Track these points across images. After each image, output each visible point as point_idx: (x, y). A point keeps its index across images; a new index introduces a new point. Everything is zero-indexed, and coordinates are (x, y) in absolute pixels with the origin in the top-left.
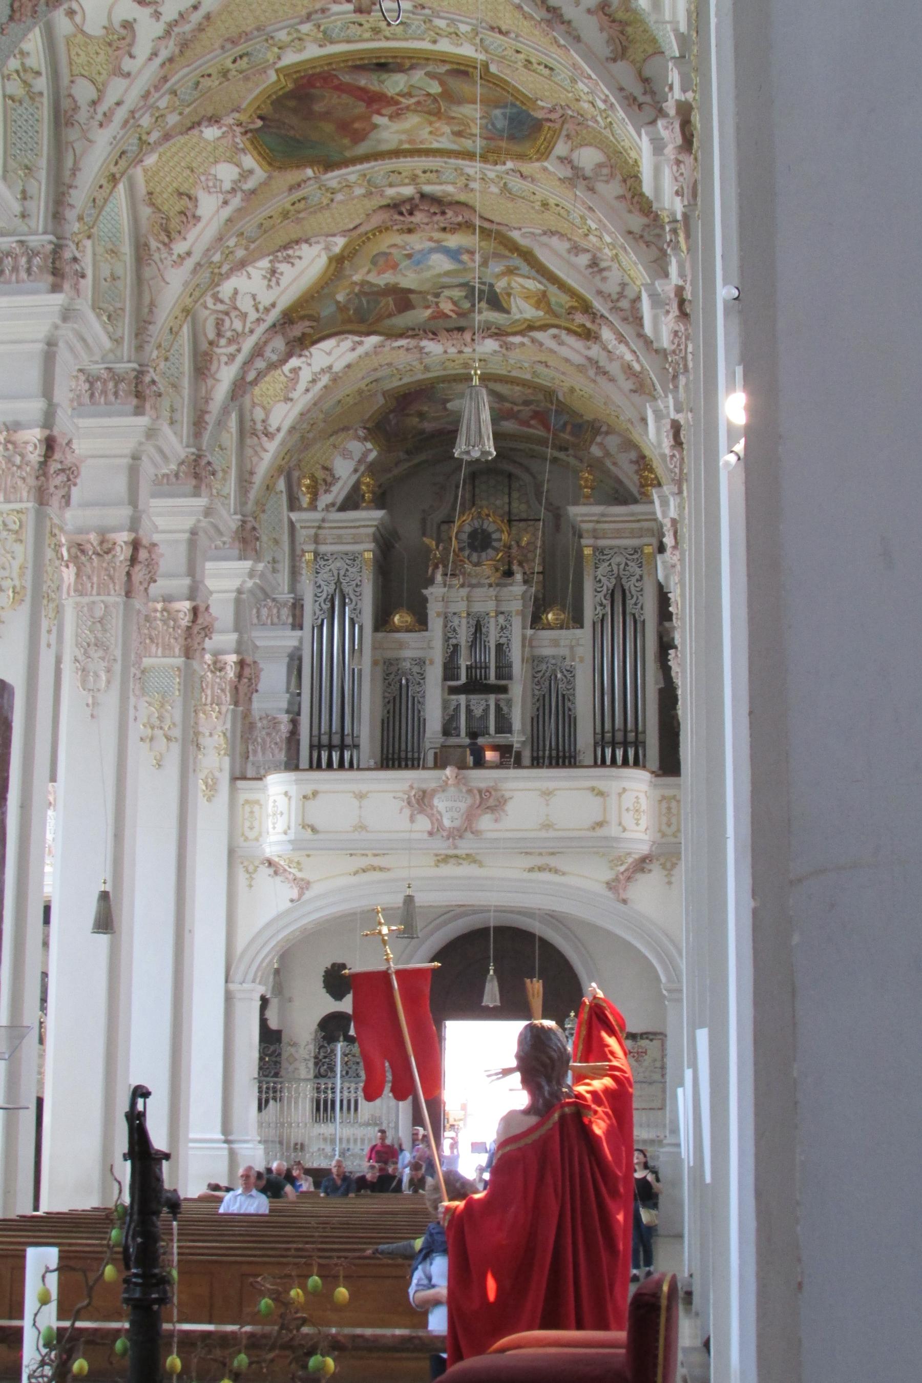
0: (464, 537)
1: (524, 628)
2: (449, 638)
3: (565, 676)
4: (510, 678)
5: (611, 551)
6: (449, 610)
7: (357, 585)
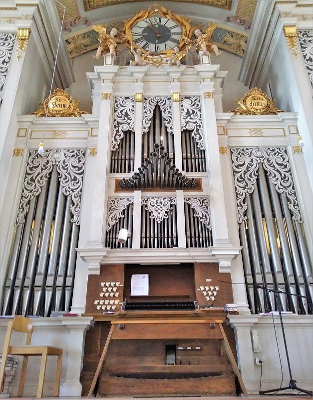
0: (140, 31)
1: (217, 111)
2: (118, 123)
3: (277, 170)
4: (203, 168)
6: (118, 94)
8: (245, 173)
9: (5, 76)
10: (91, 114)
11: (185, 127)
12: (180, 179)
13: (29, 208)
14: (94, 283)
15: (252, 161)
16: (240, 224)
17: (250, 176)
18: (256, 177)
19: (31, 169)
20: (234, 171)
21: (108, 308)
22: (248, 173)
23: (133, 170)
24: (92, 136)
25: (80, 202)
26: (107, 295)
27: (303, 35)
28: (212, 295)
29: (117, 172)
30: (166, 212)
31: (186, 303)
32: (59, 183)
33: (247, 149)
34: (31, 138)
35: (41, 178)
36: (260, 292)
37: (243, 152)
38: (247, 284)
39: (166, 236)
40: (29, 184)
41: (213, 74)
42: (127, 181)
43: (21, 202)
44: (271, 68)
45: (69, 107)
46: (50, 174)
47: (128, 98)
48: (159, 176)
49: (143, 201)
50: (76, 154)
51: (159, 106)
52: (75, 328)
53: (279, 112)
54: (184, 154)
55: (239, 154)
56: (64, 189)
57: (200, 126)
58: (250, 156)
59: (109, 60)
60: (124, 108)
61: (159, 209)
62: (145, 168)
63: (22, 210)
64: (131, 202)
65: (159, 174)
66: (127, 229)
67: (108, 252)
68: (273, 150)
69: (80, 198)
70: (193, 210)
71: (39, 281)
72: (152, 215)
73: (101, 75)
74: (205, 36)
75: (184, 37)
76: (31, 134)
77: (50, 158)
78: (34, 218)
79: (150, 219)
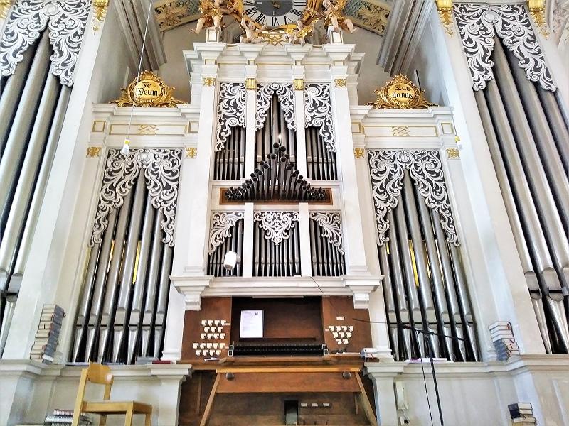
1: (351, 103)
2: (224, 116)
3: (428, 180)
4: (334, 176)
5: (476, 8)
6: (224, 79)
7: (76, 35)
8: (387, 182)
9: (77, 53)
10: (189, 103)
11: (311, 122)
12: (304, 188)
13: (107, 225)
14: (192, 320)
15: (396, 167)
16: (379, 247)
17: (393, 186)
18: (401, 188)
19: (110, 174)
20: (373, 180)
21: (211, 353)
22: (391, 183)
23: (244, 176)
24: (190, 132)
25: (174, 217)
26: (209, 336)
27: (460, 9)
28: (345, 337)
29: (223, 179)
30: (286, 231)
31: (313, 347)
32: (146, 192)
33: (389, 152)
34: (110, 134)
35: (124, 186)
36: (406, 332)
37: (384, 156)
38: (389, 323)
39: (286, 261)
40: (108, 193)
41: (346, 56)
42: (236, 190)
43: (97, 216)
44: (419, 51)
45: (161, 95)
46: (136, 180)
47: (238, 84)
48: (277, 184)
49: (256, 216)
50: (170, 155)
51: (277, 96)
52: (168, 378)
53: (430, 106)
54: (310, 157)
55: (379, 158)
56: (154, 199)
57: (329, 122)
58: (393, 161)
59: (212, 35)
60: (230, 97)
61: (277, 227)
62: (261, 173)
63: (98, 226)
64: (241, 218)
65: (275, 184)
66: (236, 251)
67: (211, 281)
68: (422, 154)
69: (175, 212)
70: (321, 228)
71: (120, 318)
72: (268, 234)
73: (202, 54)
74: (336, 7)
75: (309, 9)
76: (111, 129)
77: (135, 160)
78: (114, 237)
79: (265, 240)
